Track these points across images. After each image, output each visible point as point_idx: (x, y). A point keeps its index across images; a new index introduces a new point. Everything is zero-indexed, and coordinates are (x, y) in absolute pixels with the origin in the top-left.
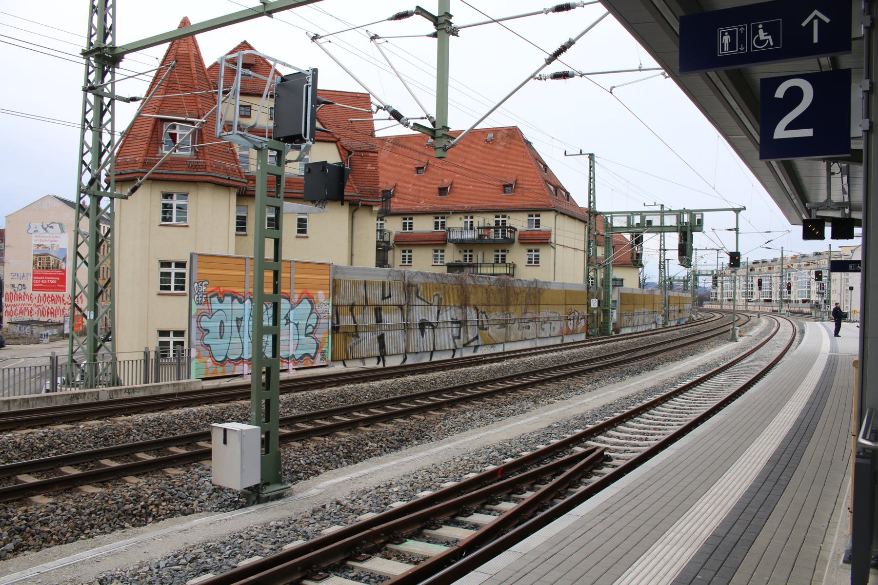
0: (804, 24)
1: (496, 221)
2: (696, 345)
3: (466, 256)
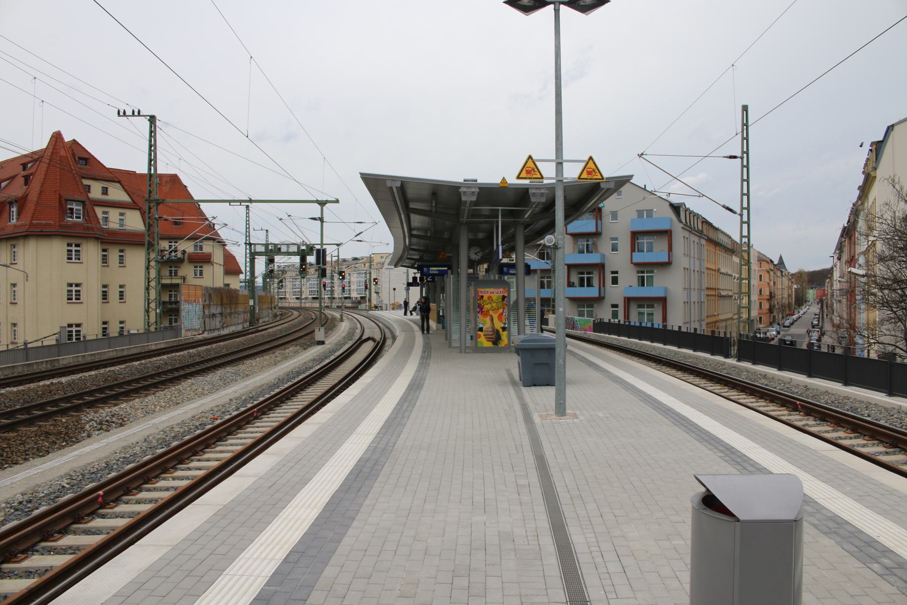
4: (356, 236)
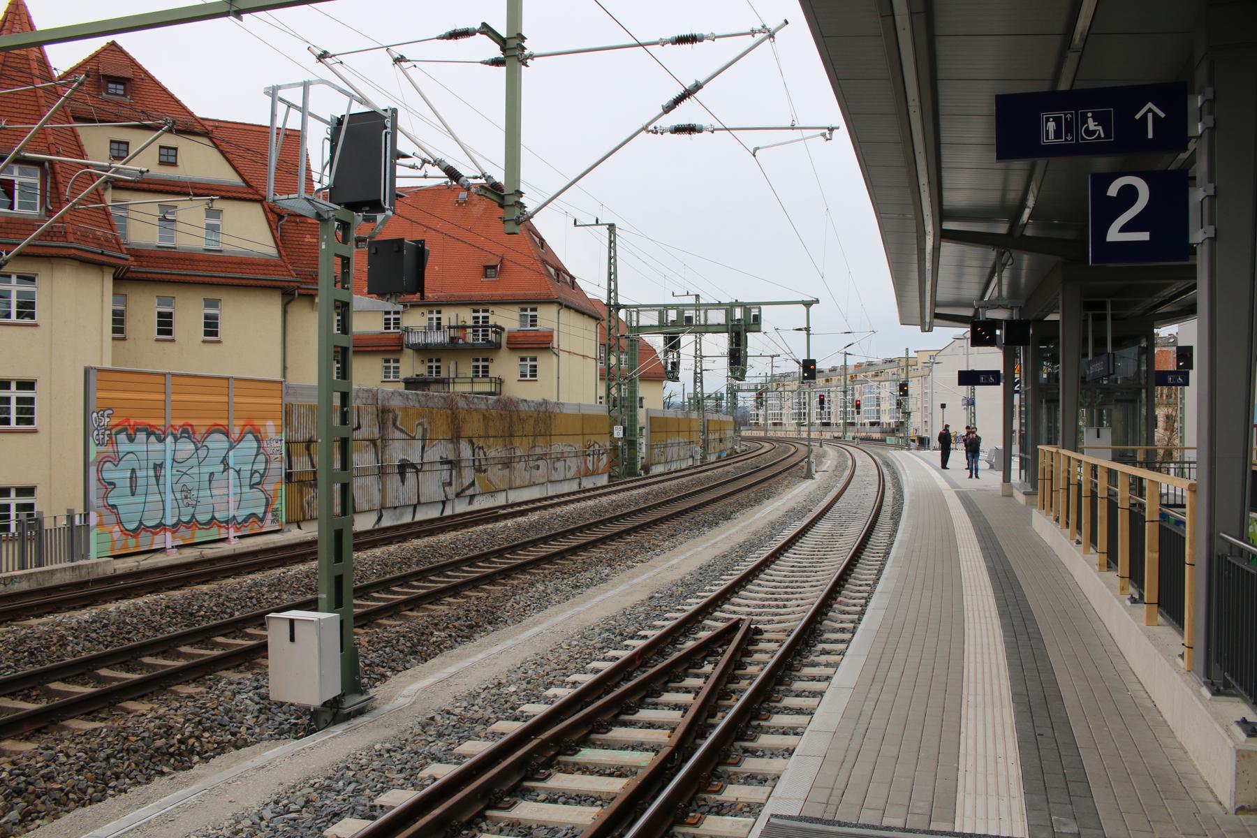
0: (1138, 117)
1: (474, 318)
2: (766, 484)
3: (431, 367)
4: (668, 109)
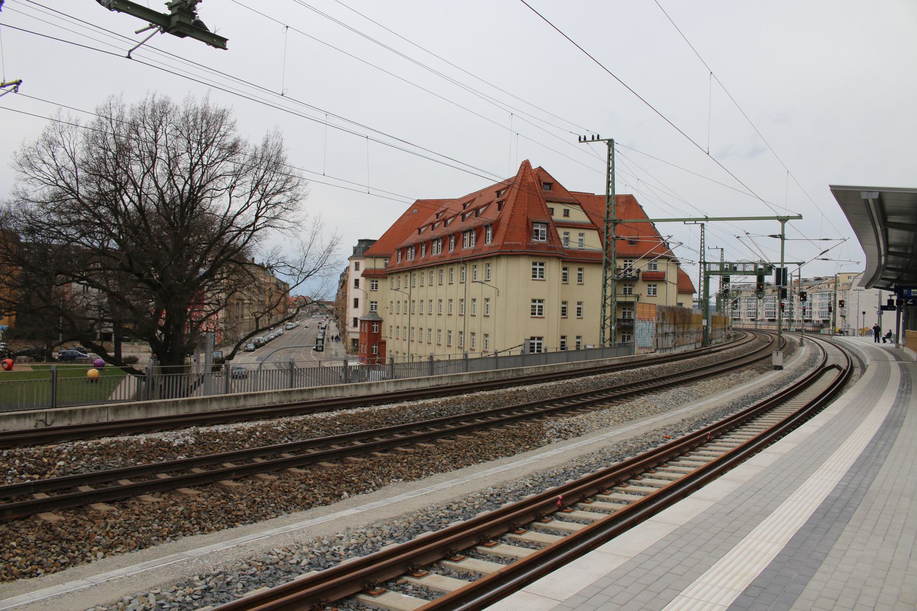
4: (821, 254)
